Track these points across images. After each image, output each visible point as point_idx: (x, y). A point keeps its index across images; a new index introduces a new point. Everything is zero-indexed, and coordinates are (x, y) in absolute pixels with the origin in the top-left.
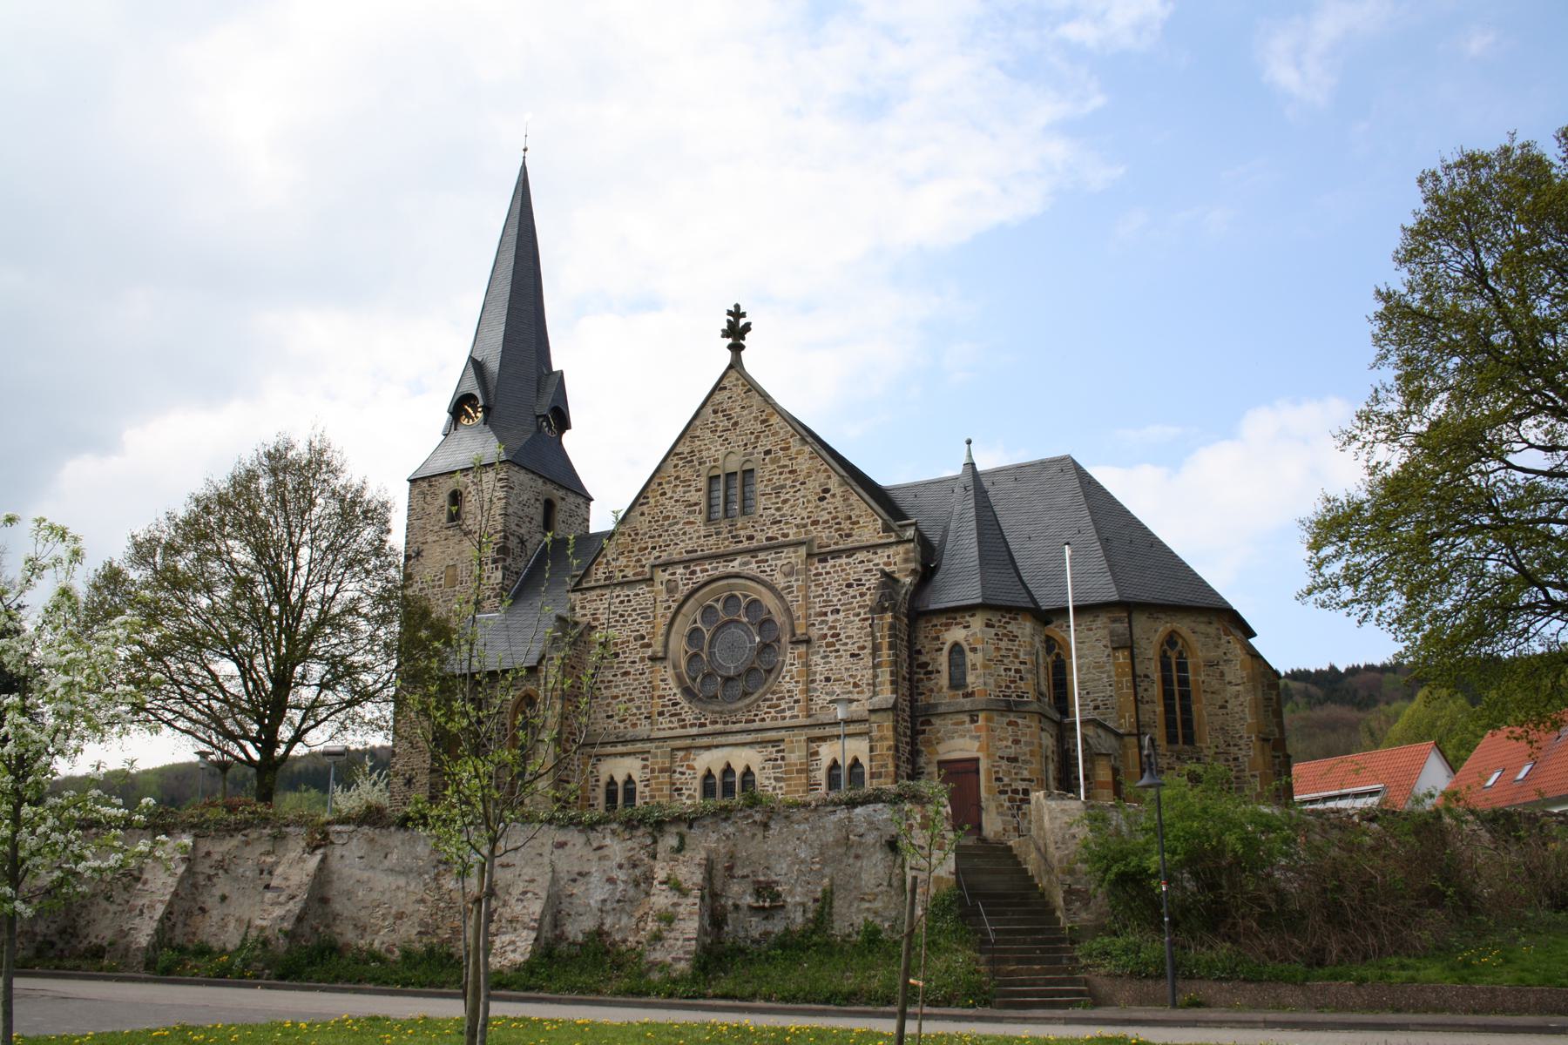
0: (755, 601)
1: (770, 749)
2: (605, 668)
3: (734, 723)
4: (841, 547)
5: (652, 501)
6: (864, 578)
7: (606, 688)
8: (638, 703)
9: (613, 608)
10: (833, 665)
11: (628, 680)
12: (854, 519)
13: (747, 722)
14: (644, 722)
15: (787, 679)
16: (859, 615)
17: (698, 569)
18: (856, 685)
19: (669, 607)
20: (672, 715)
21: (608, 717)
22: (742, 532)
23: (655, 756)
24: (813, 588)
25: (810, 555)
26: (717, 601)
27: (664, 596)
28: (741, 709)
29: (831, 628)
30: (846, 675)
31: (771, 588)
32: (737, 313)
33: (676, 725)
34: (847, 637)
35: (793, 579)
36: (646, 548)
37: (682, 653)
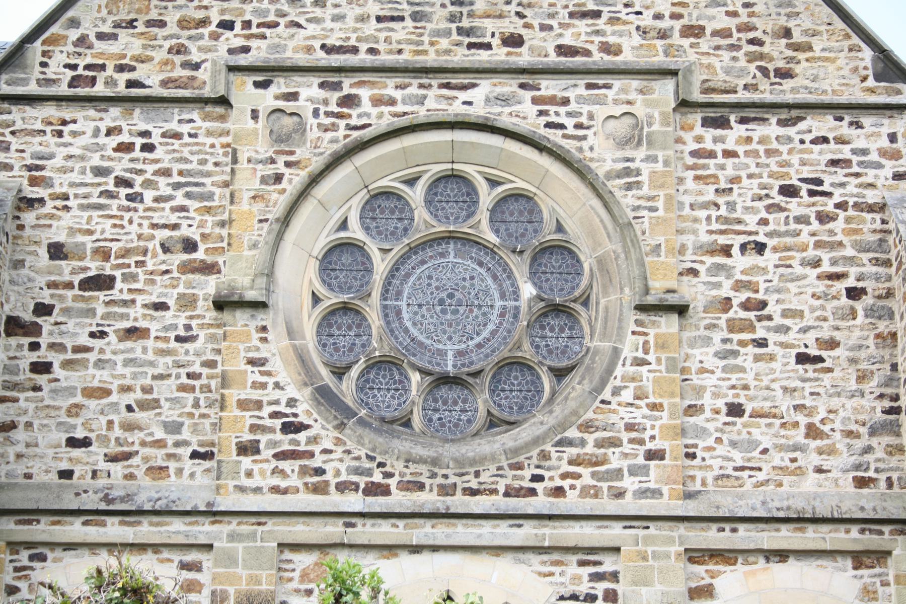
0: (517, 196)
1: (572, 569)
2: (66, 311)
3: (473, 492)
4: (768, 98)
6: (828, 180)
7: (67, 364)
8: (169, 413)
9: (96, 160)
10: (749, 378)
11: (136, 347)
12: (798, 37)
14: (189, 465)
15: (627, 395)
16: (816, 263)
17: (365, 94)
18: (812, 432)
19: (278, 178)
20: (281, 456)
21: (73, 443)
22: (489, 25)
23: (230, 560)
24: (690, 184)
25: (684, 105)
26: (411, 182)
27: (264, 149)
28: (493, 458)
29: (739, 286)
30: (785, 404)
31: (580, 171)
33: (294, 481)
34: (785, 314)
35: (641, 153)
36: (204, 22)
37: (308, 300)
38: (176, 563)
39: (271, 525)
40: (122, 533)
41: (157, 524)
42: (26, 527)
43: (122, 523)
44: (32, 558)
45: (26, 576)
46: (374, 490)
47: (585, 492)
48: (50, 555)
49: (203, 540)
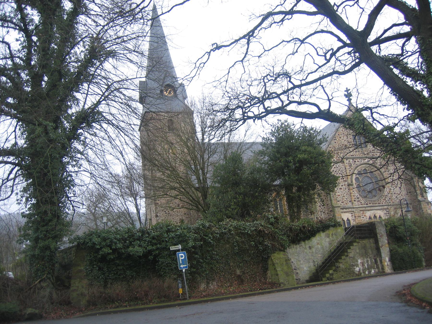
1: (385, 211)
5: (337, 139)
13: (379, 203)
14: (349, 203)
15: (386, 193)
20: (358, 201)
32: (347, 90)
39: (359, 209)
46: (367, 204)
47: (385, 203)
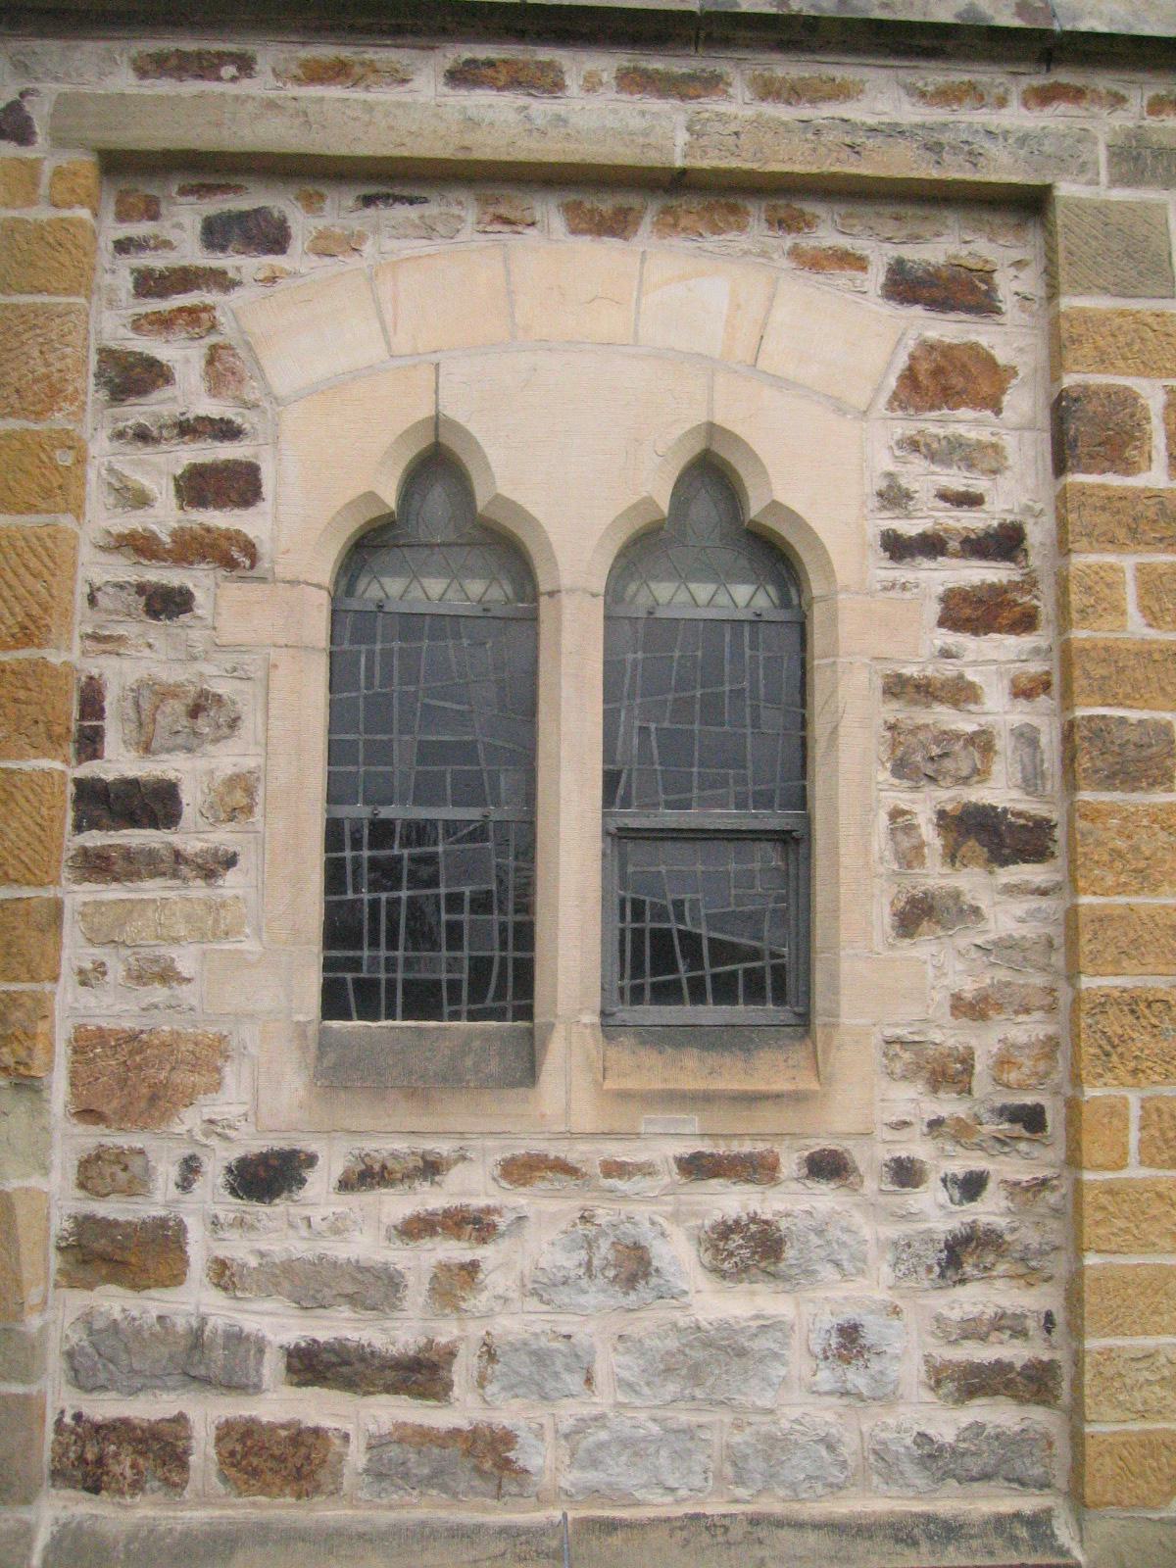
38: (875, 277)
40: (637, 123)
41: (794, 93)
42: (192, 87)
43: (633, 81)
44: (216, 233)
45: (192, 314)
48: (302, 224)
49: (1004, 169)
